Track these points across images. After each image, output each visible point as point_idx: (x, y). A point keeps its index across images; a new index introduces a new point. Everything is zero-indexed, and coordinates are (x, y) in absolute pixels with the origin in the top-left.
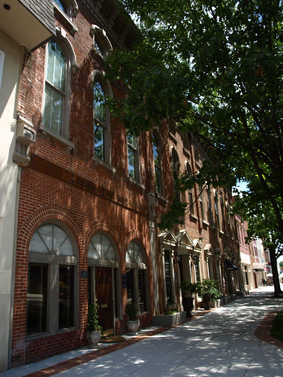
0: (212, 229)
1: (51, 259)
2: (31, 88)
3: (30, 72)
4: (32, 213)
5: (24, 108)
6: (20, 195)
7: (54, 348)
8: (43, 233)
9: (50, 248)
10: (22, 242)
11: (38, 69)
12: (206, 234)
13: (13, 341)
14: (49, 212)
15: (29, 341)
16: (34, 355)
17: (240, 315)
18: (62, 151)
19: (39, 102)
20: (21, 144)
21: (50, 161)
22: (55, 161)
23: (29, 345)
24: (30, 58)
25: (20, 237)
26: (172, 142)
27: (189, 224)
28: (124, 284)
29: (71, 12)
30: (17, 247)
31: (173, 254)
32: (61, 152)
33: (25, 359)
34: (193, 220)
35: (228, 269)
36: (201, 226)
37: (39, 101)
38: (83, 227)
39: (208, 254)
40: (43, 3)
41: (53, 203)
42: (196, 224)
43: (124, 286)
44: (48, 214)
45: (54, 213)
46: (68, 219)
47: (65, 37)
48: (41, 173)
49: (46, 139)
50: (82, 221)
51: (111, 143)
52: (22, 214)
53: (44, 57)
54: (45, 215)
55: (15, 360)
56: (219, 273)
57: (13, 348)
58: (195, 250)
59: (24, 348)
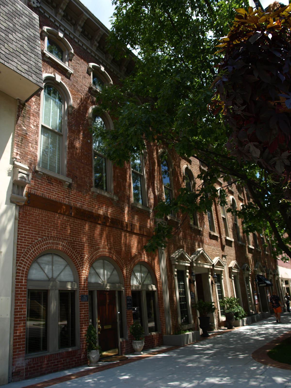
0: (239, 245)
1: (50, 286)
2: (26, 135)
3: (25, 121)
4: (30, 245)
5: (19, 154)
6: (18, 231)
7: (54, 365)
8: (43, 262)
9: (50, 276)
10: (21, 272)
11: (33, 116)
12: (231, 251)
13: (13, 359)
14: (47, 244)
15: (28, 359)
16: (33, 371)
17: (258, 333)
18: (60, 187)
19: (36, 146)
20: (18, 186)
21: (47, 197)
22: (52, 197)
23: (28, 362)
24: (24, 108)
25: (18, 267)
26: (185, 161)
27: (208, 242)
28: (129, 305)
29: (66, 56)
30: (16, 276)
31: (188, 274)
32: (58, 188)
33: (25, 374)
34: (212, 237)
35: (261, 285)
36: (224, 243)
37: (35, 144)
38: (83, 255)
39: (233, 271)
40: (30, 60)
41: (51, 234)
42: (217, 241)
43: (129, 308)
44: (46, 245)
45: (52, 244)
46: (67, 248)
47: (59, 82)
48: (38, 209)
49: (43, 178)
50: (82, 249)
51: (113, 172)
52: (20, 247)
53: (40, 103)
54: (43, 247)
55: (15, 375)
56: (249, 290)
57: (13, 365)
58: (215, 268)
59: (24, 365)
